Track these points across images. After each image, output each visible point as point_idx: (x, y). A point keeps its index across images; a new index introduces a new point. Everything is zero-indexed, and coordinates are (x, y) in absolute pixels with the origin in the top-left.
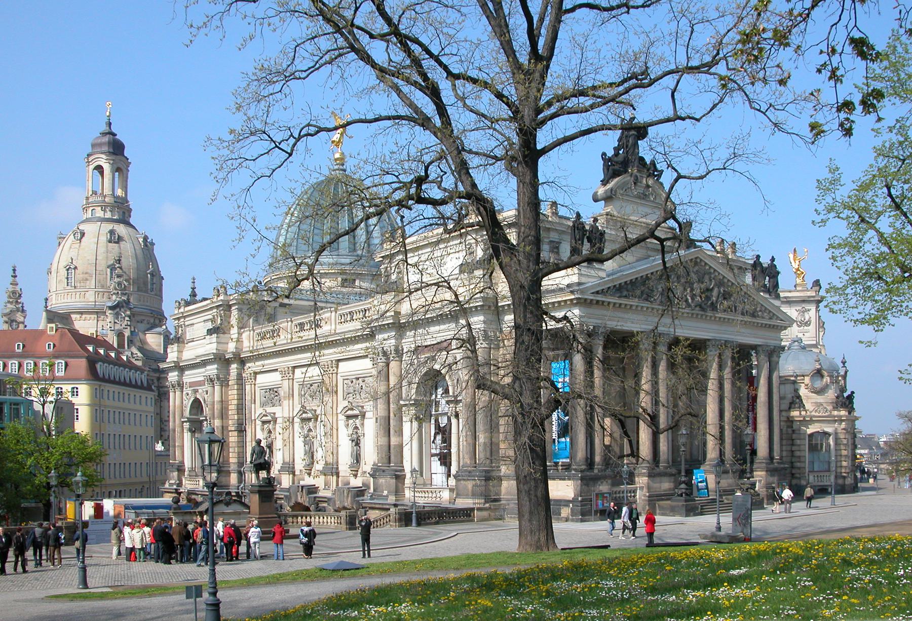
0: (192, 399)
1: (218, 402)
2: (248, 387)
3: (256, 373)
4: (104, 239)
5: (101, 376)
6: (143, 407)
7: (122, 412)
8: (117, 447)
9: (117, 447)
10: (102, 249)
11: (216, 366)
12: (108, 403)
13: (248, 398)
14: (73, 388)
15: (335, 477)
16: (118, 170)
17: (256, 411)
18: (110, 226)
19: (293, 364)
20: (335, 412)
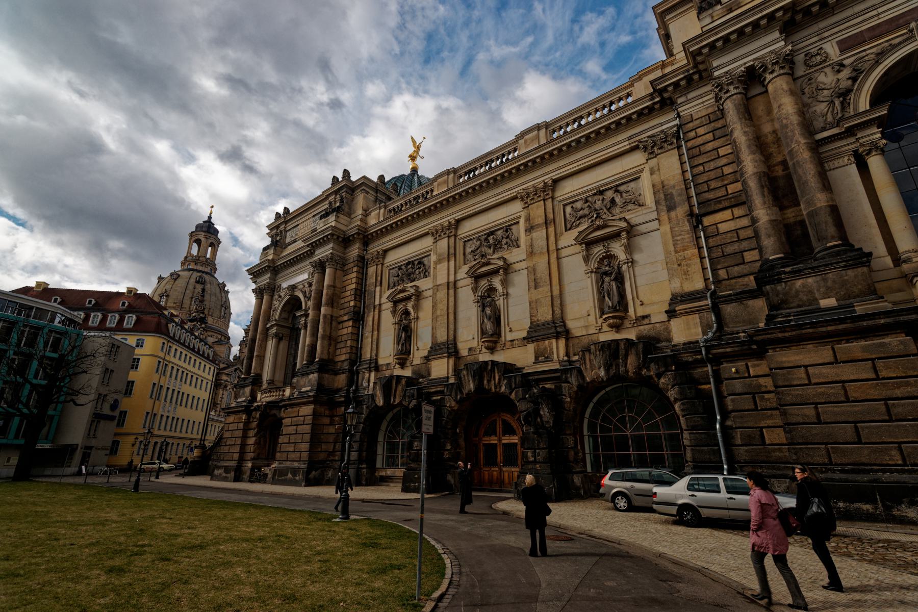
0: (288, 297)
1: (329, 286)
2: (372, 270)
3: (386, 251)
4: (193, 280)
5: (172, 335)
6: (205, 375)
7: (186, 372)
8: (174, 401)
9: (174, 401)
10: (191, 287)
11: (331, 245)
12: (172, 360)
13: (371, 280)
15: (562, 343)
16: (212, 245)
17: (382, 297)
18: (199, 274)
19: (458, 216)
20: (552, 247)
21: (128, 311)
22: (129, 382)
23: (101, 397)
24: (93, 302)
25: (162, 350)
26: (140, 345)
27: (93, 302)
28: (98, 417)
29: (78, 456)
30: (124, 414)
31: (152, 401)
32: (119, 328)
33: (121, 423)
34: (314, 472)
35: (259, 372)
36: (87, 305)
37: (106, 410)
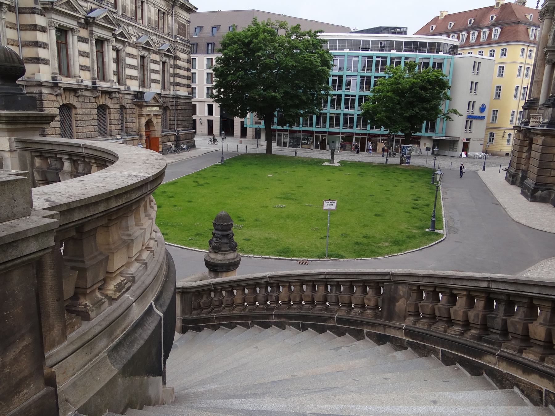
14: (503, 50)
21: (494, 25)
22: (497, 87)
23: (471, 104)
24: (473, 21)
25: (522, 55)
26: (504, 54)
27: (473, 21)
28: (471, 118)
29: (460, 146)
30: (495, 112)
31: (517, 101)
32: (489, 42)
33: (494, 119)
34: (540, 192)
35: (536, 96)
36: (469, 25)
37: (477, 113)
